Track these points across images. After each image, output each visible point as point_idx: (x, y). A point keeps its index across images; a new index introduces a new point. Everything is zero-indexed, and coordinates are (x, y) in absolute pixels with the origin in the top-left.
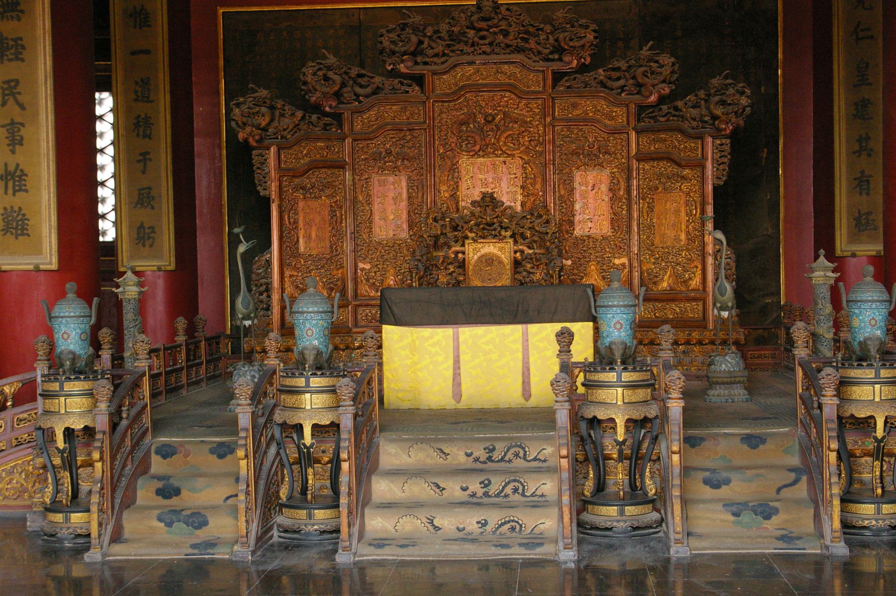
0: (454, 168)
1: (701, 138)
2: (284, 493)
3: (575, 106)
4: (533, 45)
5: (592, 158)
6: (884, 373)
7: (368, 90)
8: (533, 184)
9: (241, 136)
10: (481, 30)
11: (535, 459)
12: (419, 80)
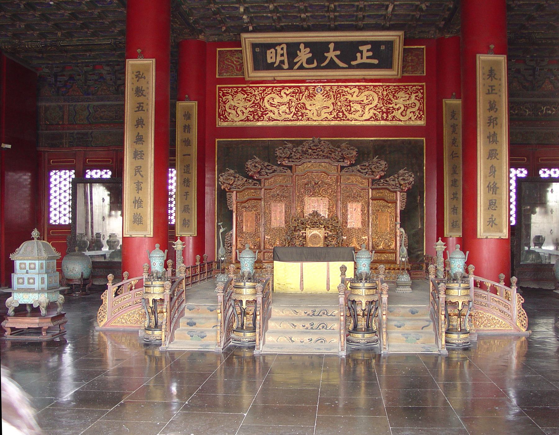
0: (302, 201)
2: (235, 326)
3: (349, 179)
4: (333, 155)
5: (355, 199)
6: (462, 285)
7: (271, 171)
8: (333, 207)
9: (222, 187)
10: (314, 149)
11: (331, 315)
12: (290, 168)
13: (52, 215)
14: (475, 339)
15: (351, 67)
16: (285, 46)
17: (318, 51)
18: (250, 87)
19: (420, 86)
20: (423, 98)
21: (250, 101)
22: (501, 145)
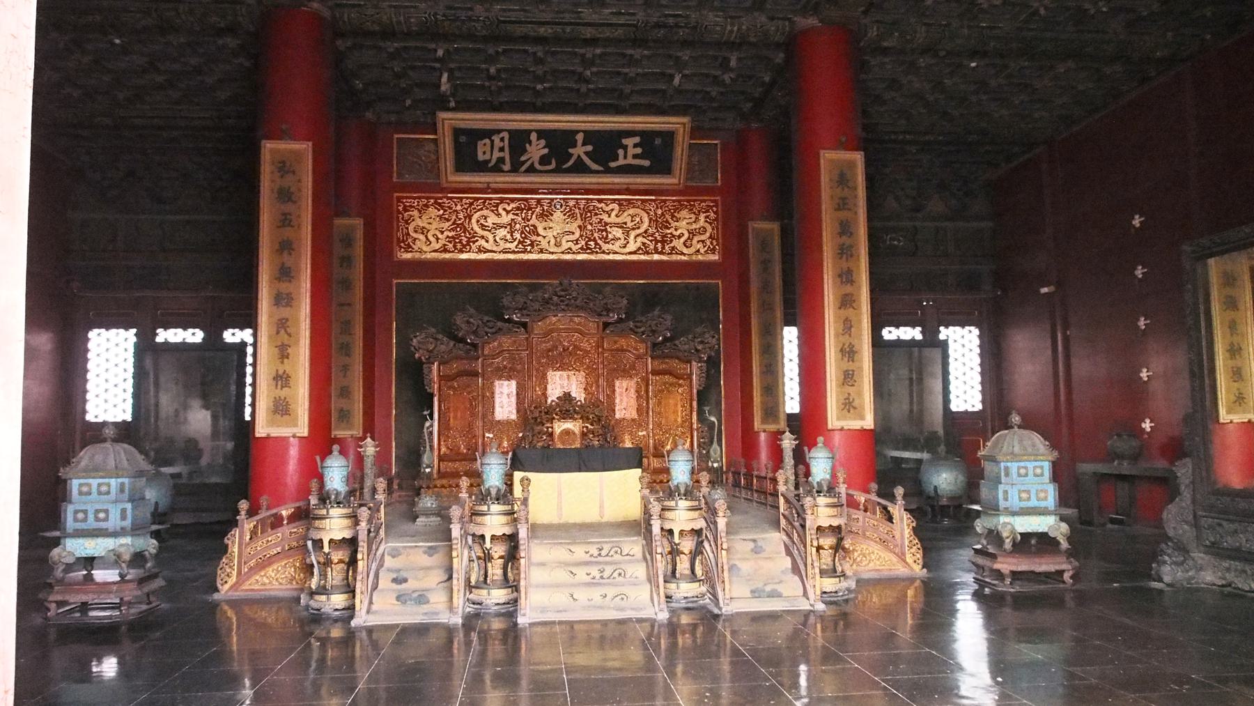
1: (690, 362)
3: (616, 342)
5: (626, 373)
12: (524, 325)
13: (89, 407)
14: (853, 585)
15: (608, 171)
16: (506, 135)
17: (559, 143)
18: (449, 198)
19: (712, 201)
20: (716, 219)
21: (448, 220)
22: (859, 288)
